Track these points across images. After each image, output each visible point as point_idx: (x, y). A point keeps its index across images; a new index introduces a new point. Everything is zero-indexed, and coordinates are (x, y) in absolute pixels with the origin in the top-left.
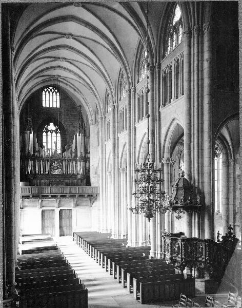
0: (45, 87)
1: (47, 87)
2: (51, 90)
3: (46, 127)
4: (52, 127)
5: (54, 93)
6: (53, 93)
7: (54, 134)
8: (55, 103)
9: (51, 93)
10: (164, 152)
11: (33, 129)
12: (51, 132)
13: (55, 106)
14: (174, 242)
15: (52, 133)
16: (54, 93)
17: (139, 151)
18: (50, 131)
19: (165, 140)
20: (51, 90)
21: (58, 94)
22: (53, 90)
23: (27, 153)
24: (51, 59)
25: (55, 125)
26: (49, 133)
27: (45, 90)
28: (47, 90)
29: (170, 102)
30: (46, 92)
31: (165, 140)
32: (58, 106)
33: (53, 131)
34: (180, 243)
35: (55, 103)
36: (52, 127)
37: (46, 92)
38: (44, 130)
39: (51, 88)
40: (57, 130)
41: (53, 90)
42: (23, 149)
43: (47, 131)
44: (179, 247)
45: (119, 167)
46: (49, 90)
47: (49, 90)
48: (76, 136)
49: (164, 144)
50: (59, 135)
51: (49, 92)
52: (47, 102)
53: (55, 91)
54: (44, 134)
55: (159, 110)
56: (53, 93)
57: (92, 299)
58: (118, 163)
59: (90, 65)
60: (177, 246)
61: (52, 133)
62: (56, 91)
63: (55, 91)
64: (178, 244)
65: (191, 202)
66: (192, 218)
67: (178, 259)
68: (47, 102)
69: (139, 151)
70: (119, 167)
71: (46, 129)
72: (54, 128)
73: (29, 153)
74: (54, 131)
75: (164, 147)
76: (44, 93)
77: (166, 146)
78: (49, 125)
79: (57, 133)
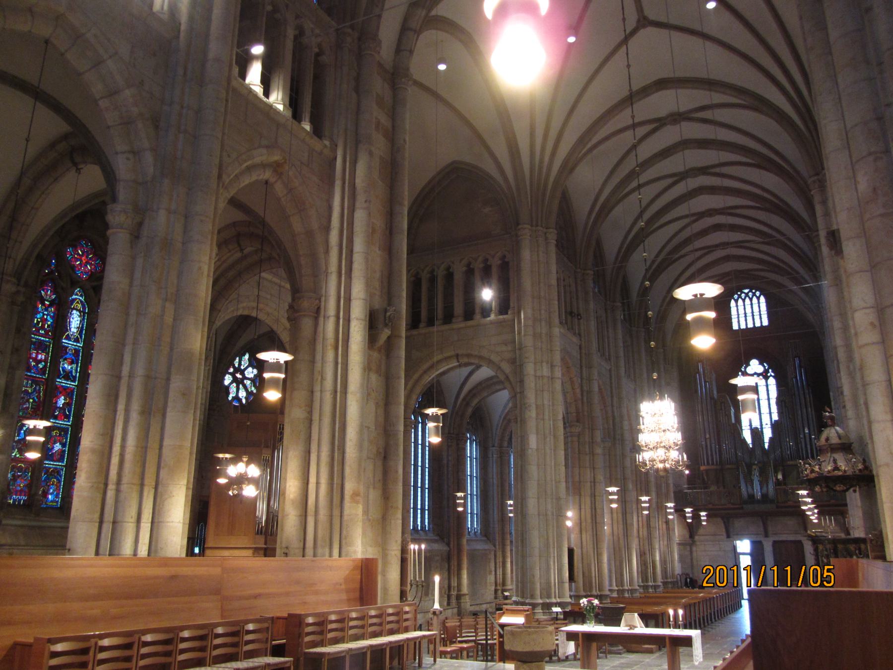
2: (747, 295)
5: (755, 300)
6: (751, 299)
8: (757, 318)
9: (747, 300)
16: (755, 300)
21: (762, 299)
22: (750, 296)
25: (761, 363)
27: (736, 296)
28: (740, 296)
30: (736, 301)
32: (766, 323)
37: (736, 301)
39: (746, 291)
40: (766, 371)
46: (743, 295)
47: (743, 295)
50: (772, 381)
51: (744, 300)
52: (742, 320)
53: (754, 294)
56: (751, 299)
62: (758, 293)
68: (742, 320)
72: (760, 369)
76: (733, 303)
78: (748, 365)
79: (766, 378)
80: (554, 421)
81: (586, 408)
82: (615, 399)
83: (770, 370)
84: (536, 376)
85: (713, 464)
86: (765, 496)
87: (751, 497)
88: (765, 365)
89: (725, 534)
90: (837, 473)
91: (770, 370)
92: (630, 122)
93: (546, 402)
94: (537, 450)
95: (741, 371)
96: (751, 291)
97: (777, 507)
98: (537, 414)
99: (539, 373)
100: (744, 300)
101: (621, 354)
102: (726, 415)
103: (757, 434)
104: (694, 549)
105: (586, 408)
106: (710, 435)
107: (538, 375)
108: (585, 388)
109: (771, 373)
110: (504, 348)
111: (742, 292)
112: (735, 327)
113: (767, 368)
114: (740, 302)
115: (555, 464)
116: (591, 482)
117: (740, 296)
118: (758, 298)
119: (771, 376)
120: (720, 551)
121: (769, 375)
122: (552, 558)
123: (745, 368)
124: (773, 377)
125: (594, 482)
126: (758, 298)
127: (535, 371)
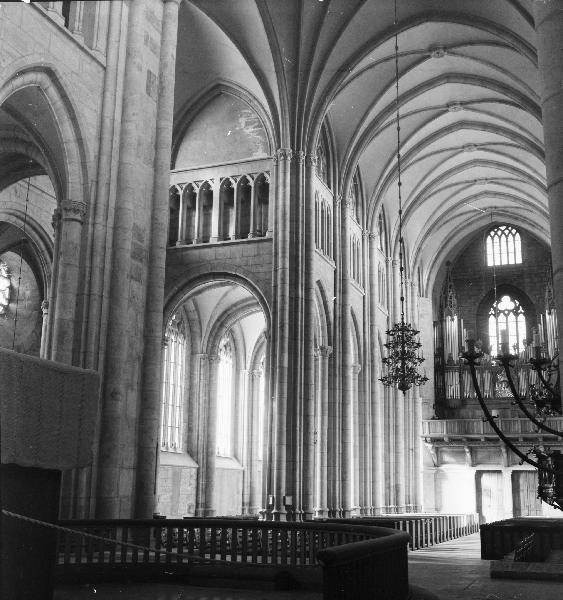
0: (508, 225)
1: (495, 226)
2: (503, 232)
4: (506, 303)
5: (510, 237)
6: (507, 236)
8: (512, 255)
11: (457, 312)
12: (505, 315)
13: (512, 262)
15: (507, 316)
16: (510, 237)
18: (503, 312)
20: (503, 232)
21: (518, 235)
23: (446, 358)
24: (460, 186)
25: (513, 300)
26: (502, 317)
27: (492, 233)
28: (496, 233)
30: (493, 238)
32: (519, 261)
33: (509, 311)
35: (512, 255)
36: (506, 303)
37: (493, 238)
38: (492, 311)
39: (503, 228)
40: (517, 308)
41: (507, 232)
42: (440, 352)
43: (496, 315)
46: (499, 233)
47: (499, 233)
48: (544, 316)
50: (522, 318)
51: (500, 237)
53: (510, 232)
54: (492, 319)
56: (507, 236)
59: (515, 177)
61: (507, 316)
62: (514, 231)
63: (510, 232)
71: (495, 309)
73: (450, 357)
74: (512, 311)
76: (489, 239)
78: (499, 301)
92: (399, 59)
96: (507, 229)
100: (500, 237)
109: (521, 310)
111: (499, 229)
112: (490, 263)
114: (496, 237)
117: (496, 233)
118: (514, 236)
124: (524, 314)
126: (514, 236)
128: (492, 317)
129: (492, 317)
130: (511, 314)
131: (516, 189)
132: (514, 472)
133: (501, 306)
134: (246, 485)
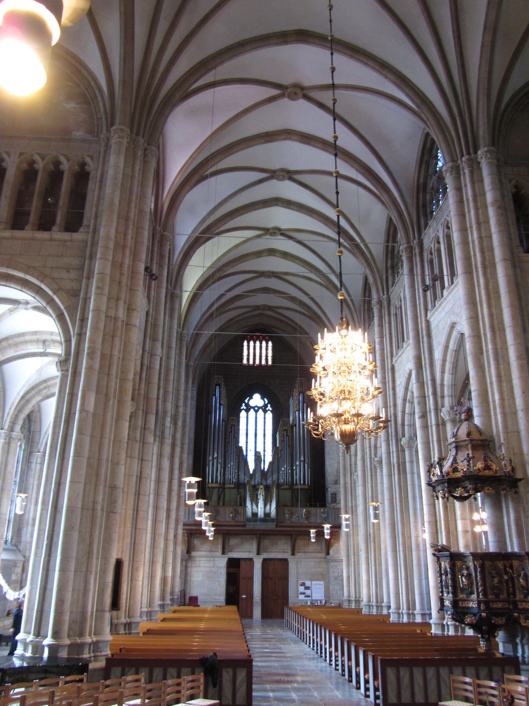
3: (246, 401)
4: (257, 400)
7: (261, 412)
10: (443, 397)
14: (459, 564)
15: (256, 411)
17: (404, 412)
18: (253, 408)
19: (443, 372)
25: (263, 398)
26: (252, 412)
29: (442, 296)
31: (443, 372)
33: (259, 408)
34: (471, 564)
36: (257, 400)
38: (244, 407)
40: (265, 406)
43: (248, 409)
44: (469, 576)
45: (373, 456)
49: (442, 380)
50: (269, 415)
54: (243, 414)
55: (426, 316)
57: (257, 666)
58: (370, 447)
60: (465, 572)
61: (256, 411)
64: (468, 568)
65: (487, 467)
66: (502, 517)
67: (471, 604)
69: (404, 412)
70: (373, 456)
71: (247, 405)
75: (442, 385)
77: (446, 383)
78: (251, 398)
79: (265, 411)
80: (121, 380)
81: (143, 386)
82: (161, 391)
83: (269, 405)
84: (107, 316)
85: (216, 482)
86: (267, 515)
87: (255, 515)
88: (265, 399)
89: (220, 550)
90: (487, 472)
91: (269, 405)
93: (116, 352)
94: (94, 414)
95: (245, 403)
97: (277, 526)
98: (101, 366)
99: (112, 313)
101: (174, 345)
102: (234, 437)
103: (258, 458)
104: (189, 564)
105: (143, 386)
106: (218, 454)
107: (109, 314)
108: (146, 362)
109: (269, 407)
110: (64, 275)
112: (245, 362)
113: (266, 403)
115: (114, 441)
116: (137, 477)
119: (269, 410)
120: (213, 567)
121: (267, 409)
122: (93, 573)
123: (249, 401)
125: (140, 478)
127: (108, 308)
128: (243, 412)
129: (243, 412)
130: (261, 410)
131: (300, 289)
132: (265, 561)
133: (252, 403)
134: (145, 574)
